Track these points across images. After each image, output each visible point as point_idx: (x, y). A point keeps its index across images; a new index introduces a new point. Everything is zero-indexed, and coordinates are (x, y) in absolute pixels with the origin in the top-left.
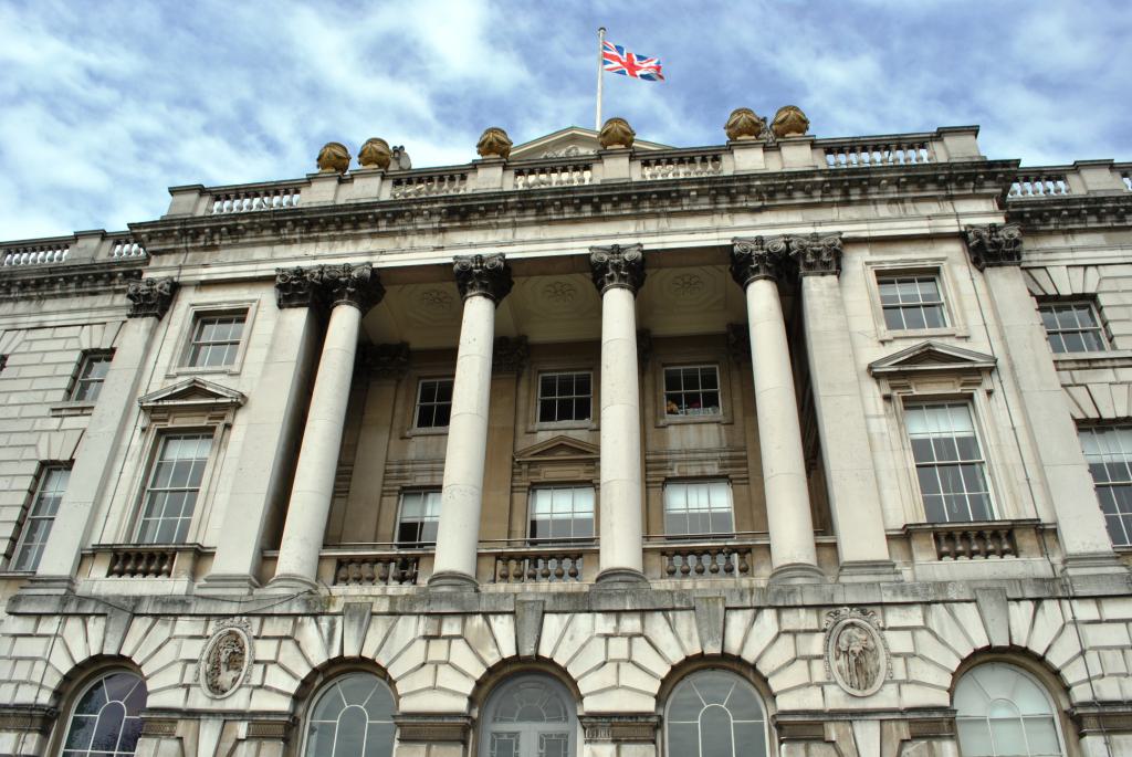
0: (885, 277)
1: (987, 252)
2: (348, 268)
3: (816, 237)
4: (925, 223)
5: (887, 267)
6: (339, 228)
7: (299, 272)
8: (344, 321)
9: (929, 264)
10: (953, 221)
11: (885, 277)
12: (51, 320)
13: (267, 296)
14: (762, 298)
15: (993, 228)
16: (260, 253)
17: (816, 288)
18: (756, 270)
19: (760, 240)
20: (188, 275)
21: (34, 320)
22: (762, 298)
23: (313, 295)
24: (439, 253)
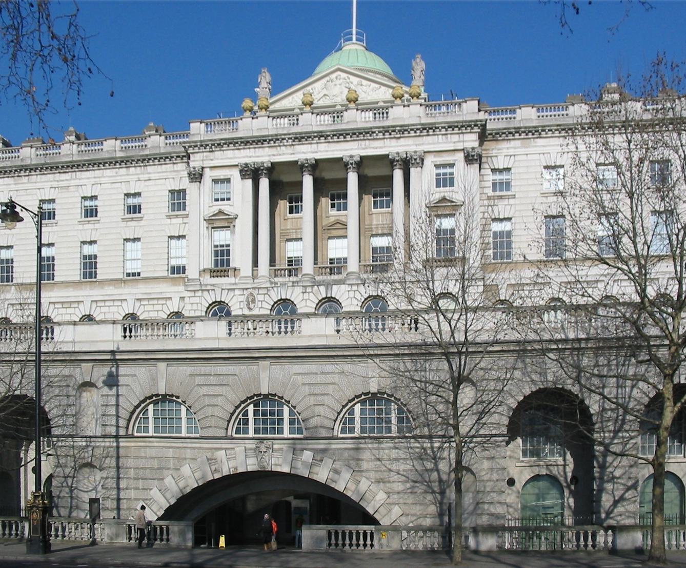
0: (437, 166)
1: (472, 158)
2: (263, 163)
3: (415, 152)
4: (452, 145)
5: (438, 163)
6: (257, 144)
7: (246, 164)
8: (264, 183)
9: (452, 162)
10: (462, 144)
11: (437, 166)
12: (153, 176)
13: (235, 174)
14: (398, 175)
15: (473, 149)
16: (230, 153)
17: (413, 171)
18: (396, 165)
19: (398, 153)
20: (206, 164)
21: (146, 177)
22: (398, 175)
23: (252, 173)
24: (293, 156)
